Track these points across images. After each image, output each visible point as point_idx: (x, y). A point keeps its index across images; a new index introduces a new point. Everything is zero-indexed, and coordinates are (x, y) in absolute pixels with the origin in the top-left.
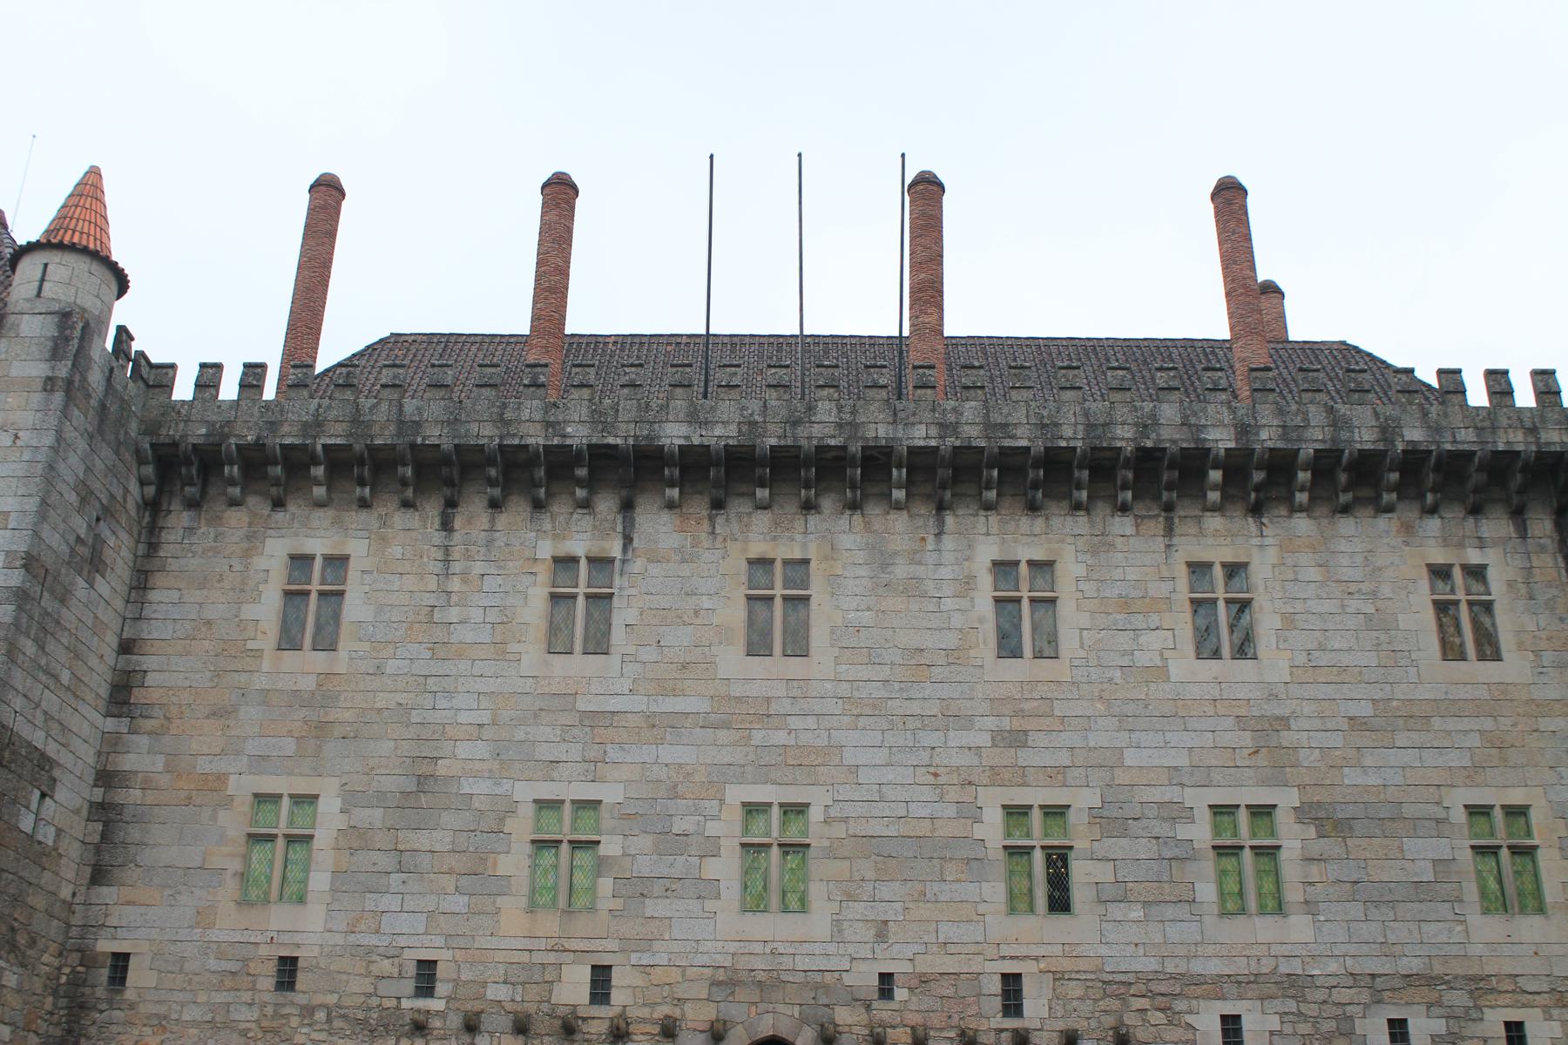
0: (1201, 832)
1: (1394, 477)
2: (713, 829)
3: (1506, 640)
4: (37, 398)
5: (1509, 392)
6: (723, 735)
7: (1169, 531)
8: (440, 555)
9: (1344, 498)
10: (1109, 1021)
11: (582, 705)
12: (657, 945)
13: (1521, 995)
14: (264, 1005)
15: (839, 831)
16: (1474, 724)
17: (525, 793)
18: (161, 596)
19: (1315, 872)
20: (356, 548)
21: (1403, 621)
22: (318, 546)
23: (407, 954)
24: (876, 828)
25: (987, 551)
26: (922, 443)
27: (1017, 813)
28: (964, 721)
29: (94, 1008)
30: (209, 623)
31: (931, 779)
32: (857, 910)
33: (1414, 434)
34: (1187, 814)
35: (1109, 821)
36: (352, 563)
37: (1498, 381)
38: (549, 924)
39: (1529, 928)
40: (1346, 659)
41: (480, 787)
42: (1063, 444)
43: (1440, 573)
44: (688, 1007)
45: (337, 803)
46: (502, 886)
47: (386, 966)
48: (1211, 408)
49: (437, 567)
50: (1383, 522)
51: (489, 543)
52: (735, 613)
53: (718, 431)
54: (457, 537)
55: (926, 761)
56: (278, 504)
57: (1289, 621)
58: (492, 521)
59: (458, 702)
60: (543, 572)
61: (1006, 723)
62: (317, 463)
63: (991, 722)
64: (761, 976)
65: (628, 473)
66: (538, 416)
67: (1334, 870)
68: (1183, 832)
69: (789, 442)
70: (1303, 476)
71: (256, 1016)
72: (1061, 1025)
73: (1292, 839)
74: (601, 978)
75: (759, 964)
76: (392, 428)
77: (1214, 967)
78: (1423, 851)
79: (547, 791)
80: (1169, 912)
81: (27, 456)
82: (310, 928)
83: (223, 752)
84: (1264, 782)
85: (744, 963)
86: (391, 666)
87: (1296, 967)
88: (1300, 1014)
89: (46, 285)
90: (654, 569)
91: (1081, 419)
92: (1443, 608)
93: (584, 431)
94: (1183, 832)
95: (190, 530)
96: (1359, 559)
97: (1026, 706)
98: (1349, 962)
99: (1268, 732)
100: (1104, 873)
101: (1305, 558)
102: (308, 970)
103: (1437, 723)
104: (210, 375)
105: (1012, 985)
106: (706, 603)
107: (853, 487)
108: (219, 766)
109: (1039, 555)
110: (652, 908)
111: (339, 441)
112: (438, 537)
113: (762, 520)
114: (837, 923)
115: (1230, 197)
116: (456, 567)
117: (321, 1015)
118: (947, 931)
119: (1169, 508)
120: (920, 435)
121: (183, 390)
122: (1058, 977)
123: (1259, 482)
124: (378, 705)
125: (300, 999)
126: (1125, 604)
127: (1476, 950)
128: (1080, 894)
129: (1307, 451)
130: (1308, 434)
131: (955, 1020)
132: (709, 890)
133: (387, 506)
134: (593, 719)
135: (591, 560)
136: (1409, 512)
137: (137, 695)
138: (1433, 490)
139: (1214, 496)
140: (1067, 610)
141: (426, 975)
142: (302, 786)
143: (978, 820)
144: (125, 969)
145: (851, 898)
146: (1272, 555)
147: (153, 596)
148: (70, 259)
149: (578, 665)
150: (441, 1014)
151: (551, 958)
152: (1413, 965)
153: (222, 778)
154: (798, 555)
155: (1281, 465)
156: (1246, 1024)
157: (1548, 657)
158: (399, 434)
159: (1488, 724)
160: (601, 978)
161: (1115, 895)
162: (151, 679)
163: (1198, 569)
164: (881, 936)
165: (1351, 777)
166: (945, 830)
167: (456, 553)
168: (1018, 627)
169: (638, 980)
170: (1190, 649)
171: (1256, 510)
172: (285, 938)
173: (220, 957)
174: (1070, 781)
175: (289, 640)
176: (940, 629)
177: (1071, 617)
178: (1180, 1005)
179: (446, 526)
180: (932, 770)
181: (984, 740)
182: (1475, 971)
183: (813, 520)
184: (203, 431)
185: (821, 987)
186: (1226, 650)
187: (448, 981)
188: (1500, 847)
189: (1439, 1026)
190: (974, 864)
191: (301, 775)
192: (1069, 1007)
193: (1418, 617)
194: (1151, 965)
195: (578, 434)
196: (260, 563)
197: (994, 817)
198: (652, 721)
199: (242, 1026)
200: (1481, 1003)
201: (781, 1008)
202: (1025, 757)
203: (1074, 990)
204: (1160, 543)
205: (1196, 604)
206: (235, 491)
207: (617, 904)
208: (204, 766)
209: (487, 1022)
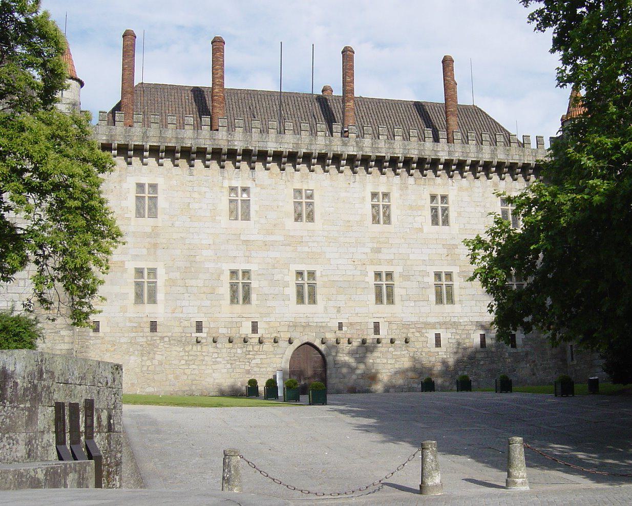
0: (431, 280)
2: (287, 278)
10: (404, 335)
11: (242, 238)
12: (271, 315)
14: (147, 337)
15: (325, 279)
17: (227, 267)
22: (146, 180)
24: (336, 278)
25: (370, 189)
26: (351, 153)
27: (378, 275)
29: (90, 339)
31: (353, 263)
32: (331, 303)
36: (159, 187)
38: (239, 308)
41: (210, 265)
42: (396, 155)
44: (282, 334)
47: (186, 323)
48: (440, 145)
49: (190, 189)
55: (351, 257)
57: (459, 214)
60: (226, 192)
62: (146, 151)
63: (370, 245)
64: (303, 324)
66: (225, 138)
68: (426, 279)
69: (309, 151)
70: (467, 168)
71: (145, 340)
72: (391, 337)
75: (303, 320)
76: (174, 140)
77: (432, 320)
79: (234, 267)
80: (422, 303)
82: (159, 311)
84: (449, 265)
85: (298, 320)
86: (177, 224)
88: (456, 333)
91: (402, 147)
94: (426, 279)
96: (481, 194)
97: (381, 240)
98: (471, 318)
100: (403, 292)
109: (385, 191)
110: (269, 303)
111: (155, 144)
114: (325, 307)
115: (447, 63)
117: (166, 339)
120: (351, 150)
122: (390, 323)
124: (174, 238)
125: (159, 334)
126: (411, 207)
128: (397, 298)
129: (469, 162)
130: (470, 155)
131: (360, 336)
132: (287, 298)
134: (246, 242)
135: (241, 187)
141: (199, 327)
143: (366, 275)
149: (240, 224)
150: (206, 338)
151: (239, 320)
153: (123, 262)
155: (461, 165)
158: (177, 143)
164: (339, 311)
168: (378, 214)
169: (267, 326)
172: (152, 315)
173: (130, 321)
174: (394, 264)
175: (139, 214)
176: (355, 214)
177: (395, 213)
178: (424, 331)
179: (191, 174)
180: (353, 260)
181: (368, 250)
184: (105, 138)
185: (322, 327)
186: (441, 222)
187: (206, 328)
191: (150, 261)
192: (393, 332)
195: (239, 146)
196: (125, 186)
199: (141, 343)
201: (309, 333)
202: (381, 256)
205: (433, 209)
209: (219, 340)
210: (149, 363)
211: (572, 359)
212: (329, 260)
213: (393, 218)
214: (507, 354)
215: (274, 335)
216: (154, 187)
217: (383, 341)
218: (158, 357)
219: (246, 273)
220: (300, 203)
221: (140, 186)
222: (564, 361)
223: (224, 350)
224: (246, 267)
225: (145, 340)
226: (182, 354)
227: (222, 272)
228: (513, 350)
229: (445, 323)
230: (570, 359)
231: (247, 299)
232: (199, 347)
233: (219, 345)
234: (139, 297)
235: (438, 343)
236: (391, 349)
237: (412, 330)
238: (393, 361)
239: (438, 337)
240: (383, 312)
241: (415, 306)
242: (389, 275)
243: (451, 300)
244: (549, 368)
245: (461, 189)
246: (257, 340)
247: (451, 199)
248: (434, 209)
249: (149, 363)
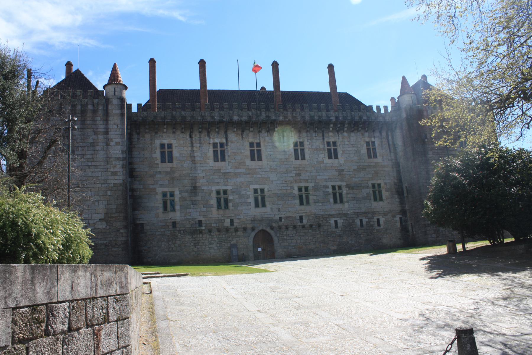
0: (330, 190)
2: (248, 193)
3: (378, 154)
4: (120, 118)
5: (380, 110)
6: (248, 176)
7: (323, 135)
8: (190, 142)
9: (353, 129)
11: (222, 171)
15: (270, 193)
17: (214, 188)
18: (135, 153)
19: (348, 196)
20: (173, 142)
21: (362, 152)
22: (166, 142)
23: (196, 220)
28: (290, 172)
30: (146, 158)
33: (365, 118)
34: (328, 187)
35: (315, 189)
37: (378, 107)
38: (221, 212)
39: (381, 203)
40: (353, 159)
43: (368, 143)
45: (178, 193)
46: (212, 206)
47: (193, 222)
50: (359, 133)
51: (200, 140)
52: (248, 153)
53: (244, 118)
54: (194, 139)
56: (156, 133)
57: (344, 152)
58: (200, 136)
59: (198, 172)
60: (212, 147)
61: (297, 172)
62: (165, 125)
63: (295, 172)
65: (226, 125)
67: (351, 195)
68: (328, 190)
70: (346, 125)
71: (170, 232)
73: (345, 191)
74: (232, 221)
75: (259, 217)
77: (333, 213)
78: (365, 191)
79: (218, 188)
80: (326, 204)
81: (121, 130)
82: (177, 216)
83: (154, 184)
87: (346, 212)
89: (116, 93)
90: (232, 145)
92: (368, 150)
93: (219, 118)
94: (328, 190)
95: (138, 139)
99: (340, 171)
100: (315, 198)
101: (346, 140)
102: (178, 224)
104: (139, 105)
105: (301, 217)
106: (243, 151)
107: (268, 127)
108: (155, 186)
109: (301, 140)
110: (239, 208)
112: (189, 139)
113: (251, 134)
114: (272, 209)
116: (195, 145)
118: (290, 209)
119: (323, 131)
121: (134, 109)
122: (309, 216)
123: (339, 126)
125: (178, 229)
126: (316, 150)
127: (373, 207)
128: (311, 202)
132: (249, 204)
133: (178, 132)
134: (224, 174)
137: (135, 173)
139: (331, 129)
140: (306, 151)
142: (171, 189)
144: (143, 226)
145: (273, 204)
146: (340, 139)
147: (134, 153)
148: (119, 86)
149: (220, 164)
152: (363, 210)
153: (155, 189)
154: (258, 141)
155: (343, 124)
156: (339, 222)
159: (375, 169)
160: (232, 221)
161: (315, 202)
162: (137, 170)
163: (328, 144)
164: (279, 210)
165: (354, 179)
166: (289, 191)
167: (194, 142)
170: (327, 158)
171: (338, 131)
175: (163, 161)
177: (307, 152)
178: (328, 219)
181: (294, 175)
183: (261, 134)
186: (333, 157)
189: (367, 220)
190: (294, 197)
193: (364, 151)
194: (322, 213)
197: (296, 189)
198: (235, 174)
202: (301, 178)
203: (311, 218)
204: (321, 138)
205: (328, 149)
206: (147, 131)
207: (233, 208)
208: (151, 187)
210: (173, 246)
212: (272, 181)
213: (307, 156)
214: (375, 231)
215: (244, 226)
216: (170, 146)
217: (306, 226)
218: (178, 242)
219: (225, 192)
220: (254, 150)
221: (162, 146)
223: (215, 236)
224: (225, 188)
225: (170, 232)
226: (191, 240)
227: (212, 191)
228: (378, 228)
229: (340, 214)
231: (227, 207)
232: (201, 236)
233: (212, 234)
234: (165, 209)
235: (336, 226)
236: (310, 231)
237: (321, 219)
238: (311, 238)
239: (336, 222)
240: (304, 210)
241: (322, 205)
242: (306, 189)
243: (342, 201)
245: (343, 138)
246: (233, 230)
247: (338, 144)
248: (329, 151)
249: (173, 246)
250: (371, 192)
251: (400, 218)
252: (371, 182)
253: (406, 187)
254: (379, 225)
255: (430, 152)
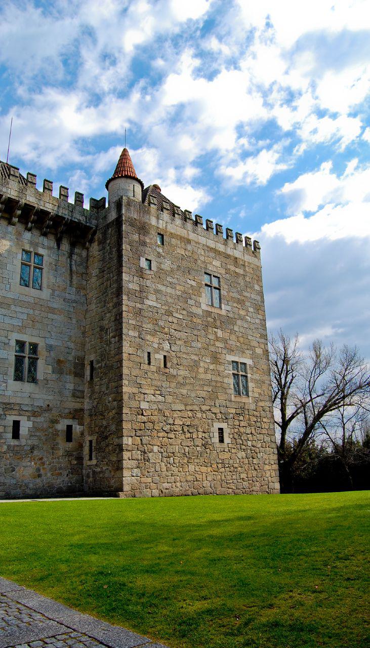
1: (19, 212)
13: (21, 411)
16: (26, 311)
39: (28, 387)
50: (10, 228)
103: (13, 307)
127: (7, 393)
136: (20, 227)
138: (32, 223)
157: (57, 293)
159: (31, 312)
182: (6, 401)
188: (25, 357)
200: (7, 413)
211: (91, 459)
214: (5, 447)
222: (80, 459)
228: (14, 442)
230: (87, 457)
244: (60, 468)
250: (12, 360)
251: (69, 428)
252: (15, 336)
253: (92, 362)
254: (16, 435)
255: (152, 297)
